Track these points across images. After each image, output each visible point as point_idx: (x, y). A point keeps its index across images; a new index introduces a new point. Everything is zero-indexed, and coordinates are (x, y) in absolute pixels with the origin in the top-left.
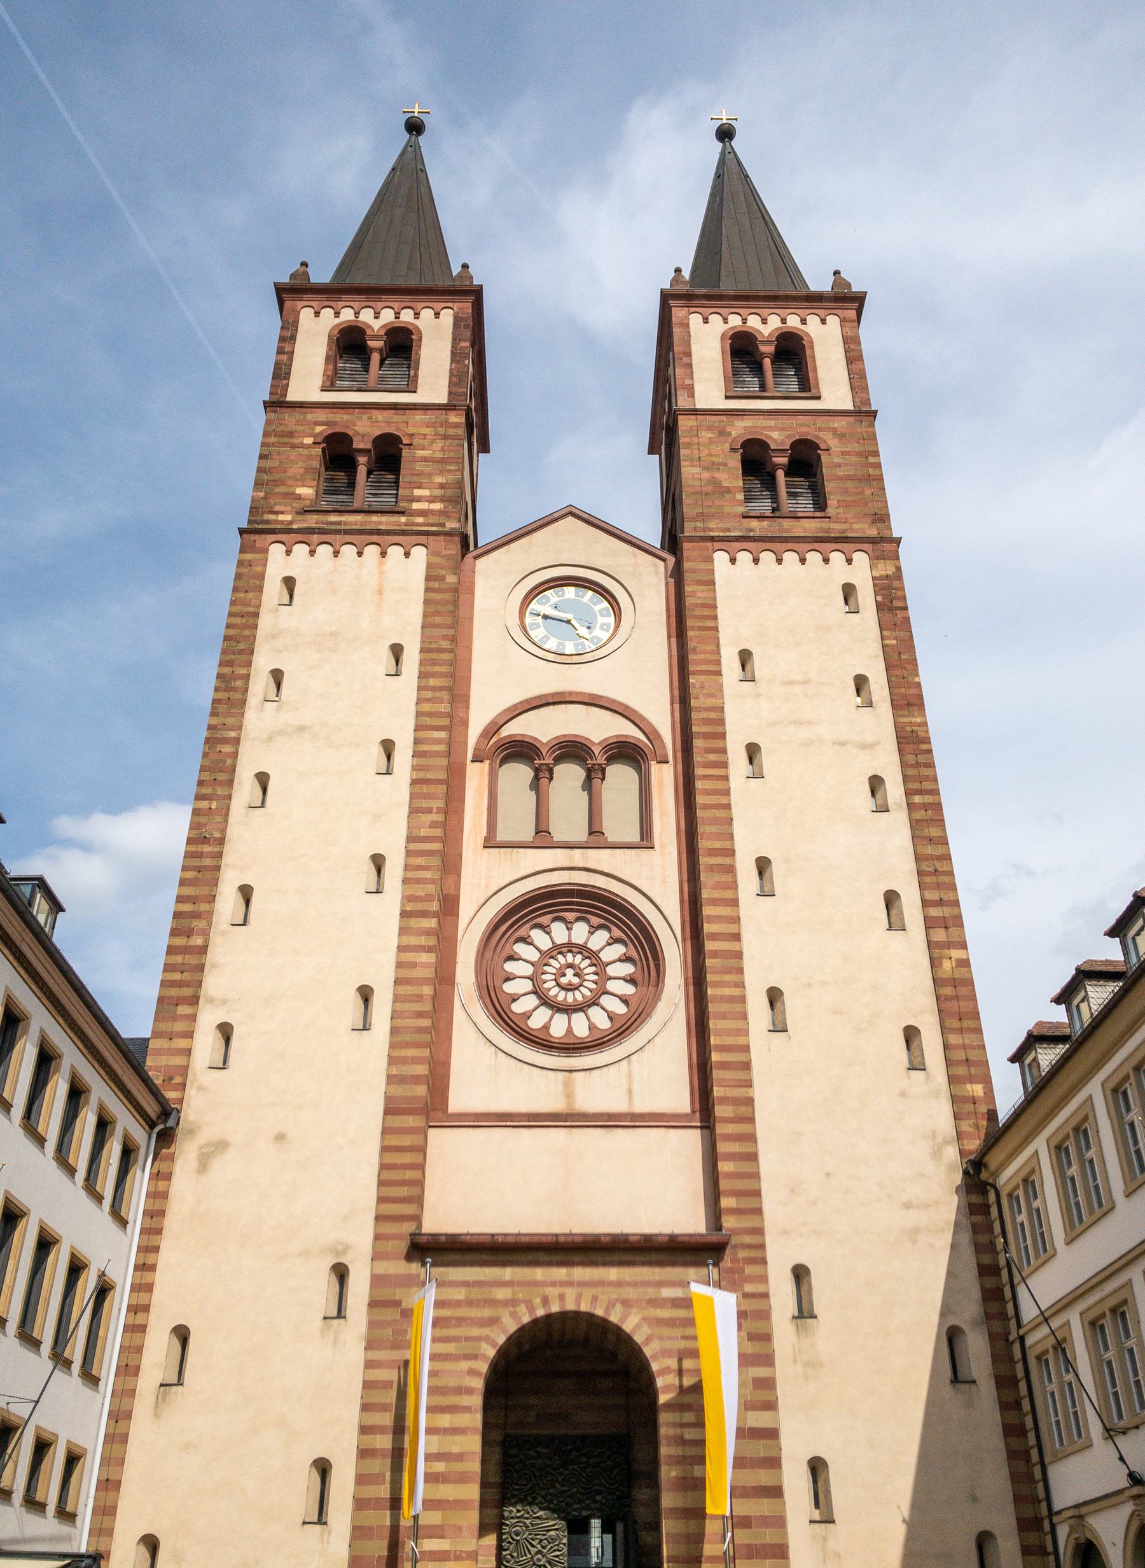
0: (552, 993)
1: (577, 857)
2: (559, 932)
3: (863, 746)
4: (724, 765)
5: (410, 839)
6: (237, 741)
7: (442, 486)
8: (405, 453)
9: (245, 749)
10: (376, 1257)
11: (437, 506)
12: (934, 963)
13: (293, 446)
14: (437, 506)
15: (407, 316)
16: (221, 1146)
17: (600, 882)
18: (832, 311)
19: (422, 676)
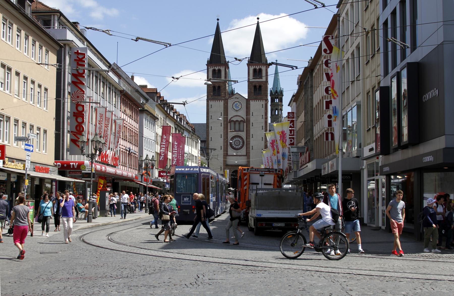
0: (236, 138)
1: (238, 132)
3: (262, 123)
4: (250, 125)
5: (224, 133)
6: (209, 123)
7: (225, 92)
8: (221, 88)
9: (210, 124)
10: (224, 166)
11: (224, 95)
12: (265, 144)
13: (210, 88)
14: (224, 95)
15: (220, 68)
17: (239, 135)
18: (265, 65)
19: (224, 116)
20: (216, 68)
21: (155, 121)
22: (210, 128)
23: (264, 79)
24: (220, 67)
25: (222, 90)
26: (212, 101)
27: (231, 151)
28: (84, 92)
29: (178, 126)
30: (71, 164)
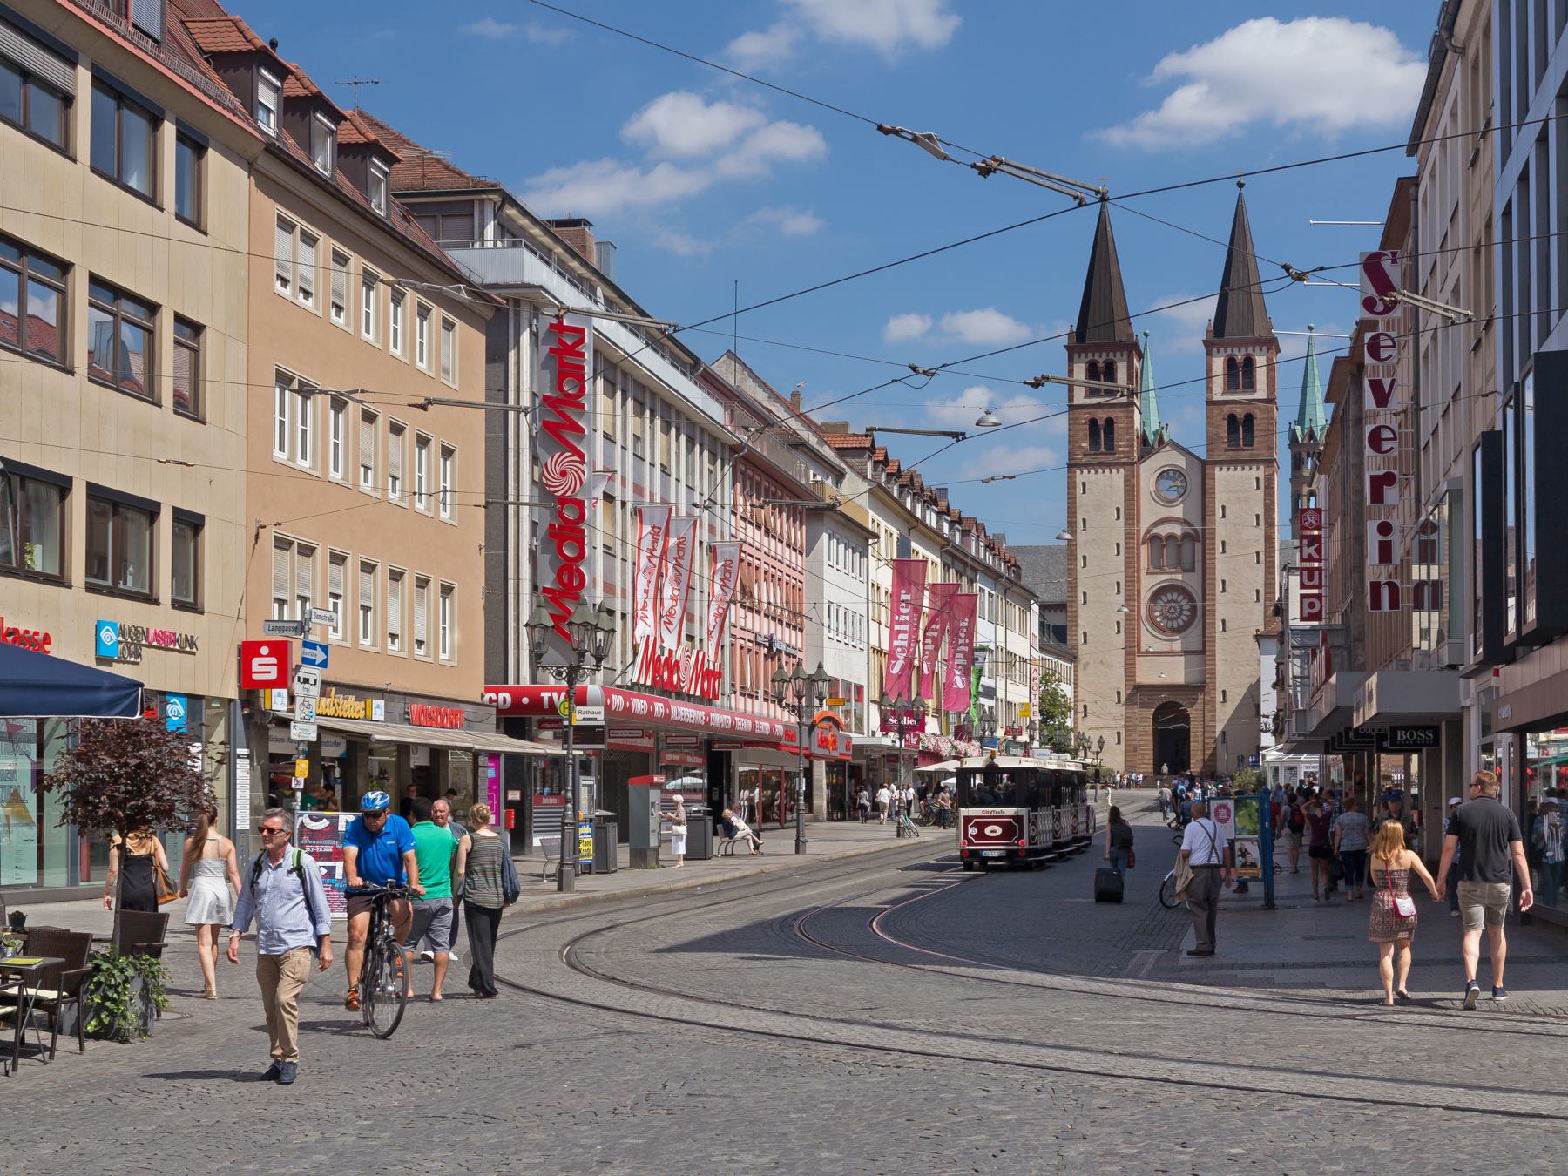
2: (1169, 597)
16: (1088, 664)
20: (1097, 357)
21: (868, 545)
22: (1080, 562)
23: (1261, 392)
24: (1111, 354)
25: (1120, 432)
26: (1085, 471)
27: (1149, 640)
28: (581, 456)
29: (954, 557)
30: (546, 695)
